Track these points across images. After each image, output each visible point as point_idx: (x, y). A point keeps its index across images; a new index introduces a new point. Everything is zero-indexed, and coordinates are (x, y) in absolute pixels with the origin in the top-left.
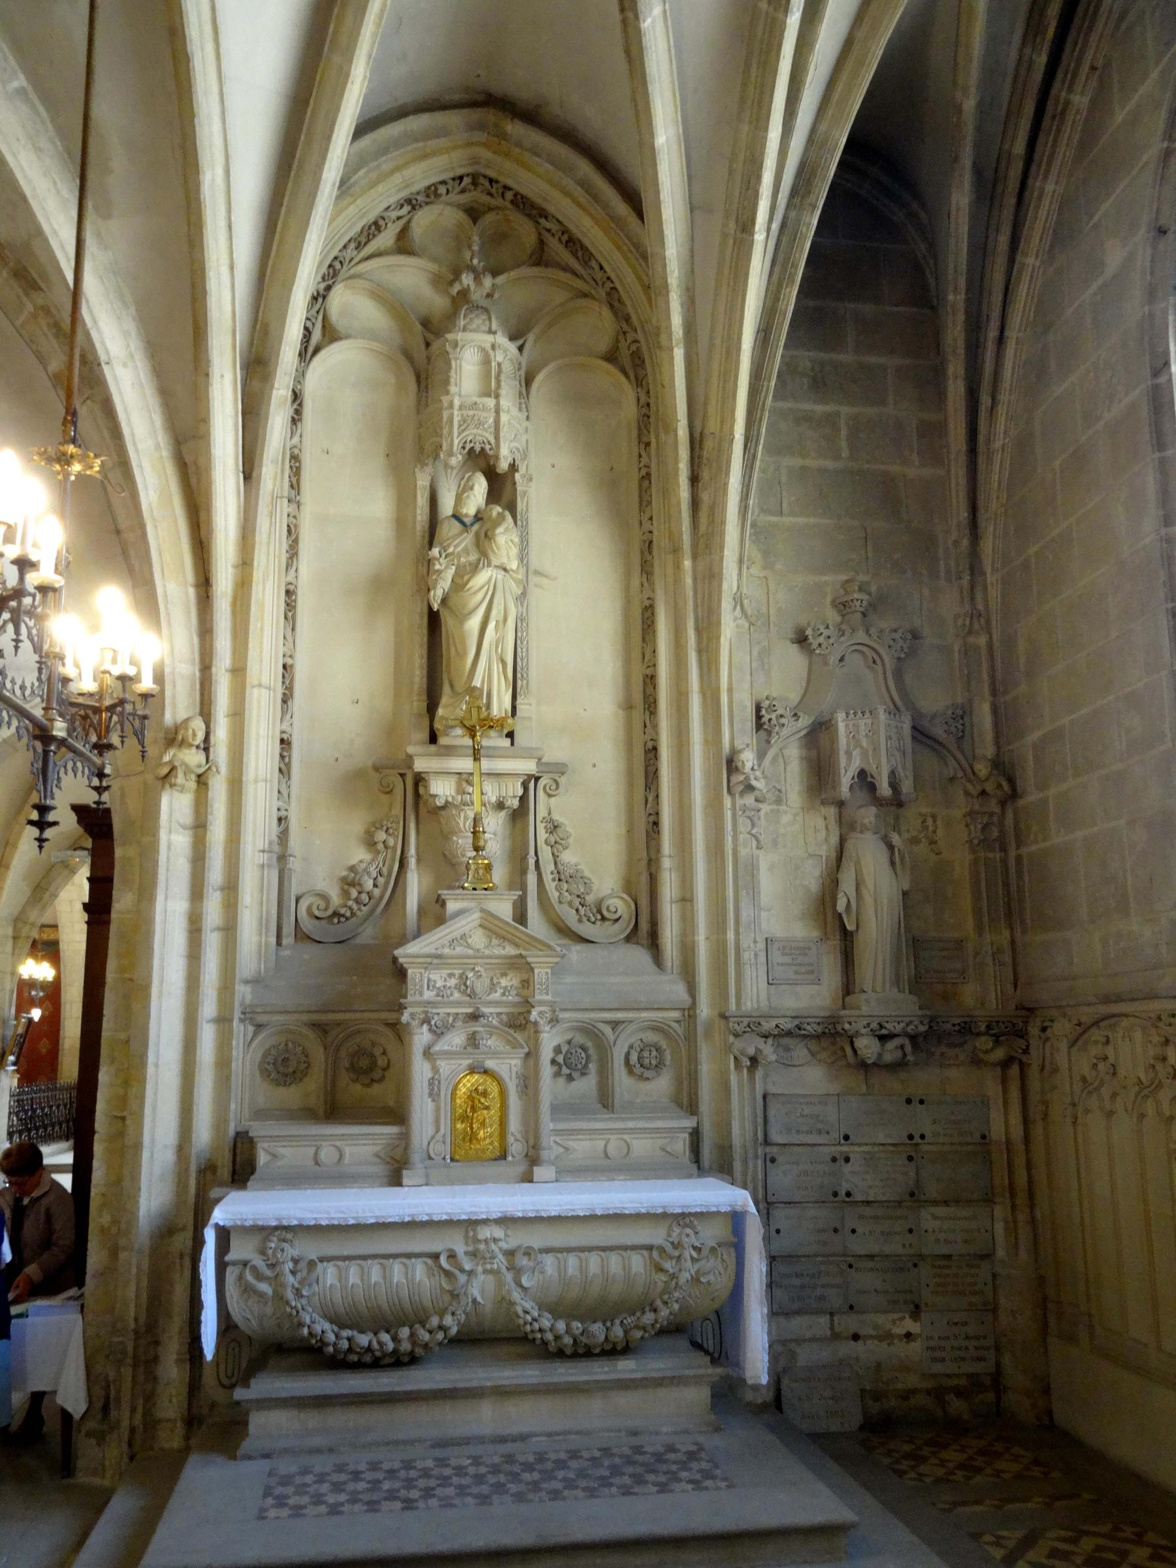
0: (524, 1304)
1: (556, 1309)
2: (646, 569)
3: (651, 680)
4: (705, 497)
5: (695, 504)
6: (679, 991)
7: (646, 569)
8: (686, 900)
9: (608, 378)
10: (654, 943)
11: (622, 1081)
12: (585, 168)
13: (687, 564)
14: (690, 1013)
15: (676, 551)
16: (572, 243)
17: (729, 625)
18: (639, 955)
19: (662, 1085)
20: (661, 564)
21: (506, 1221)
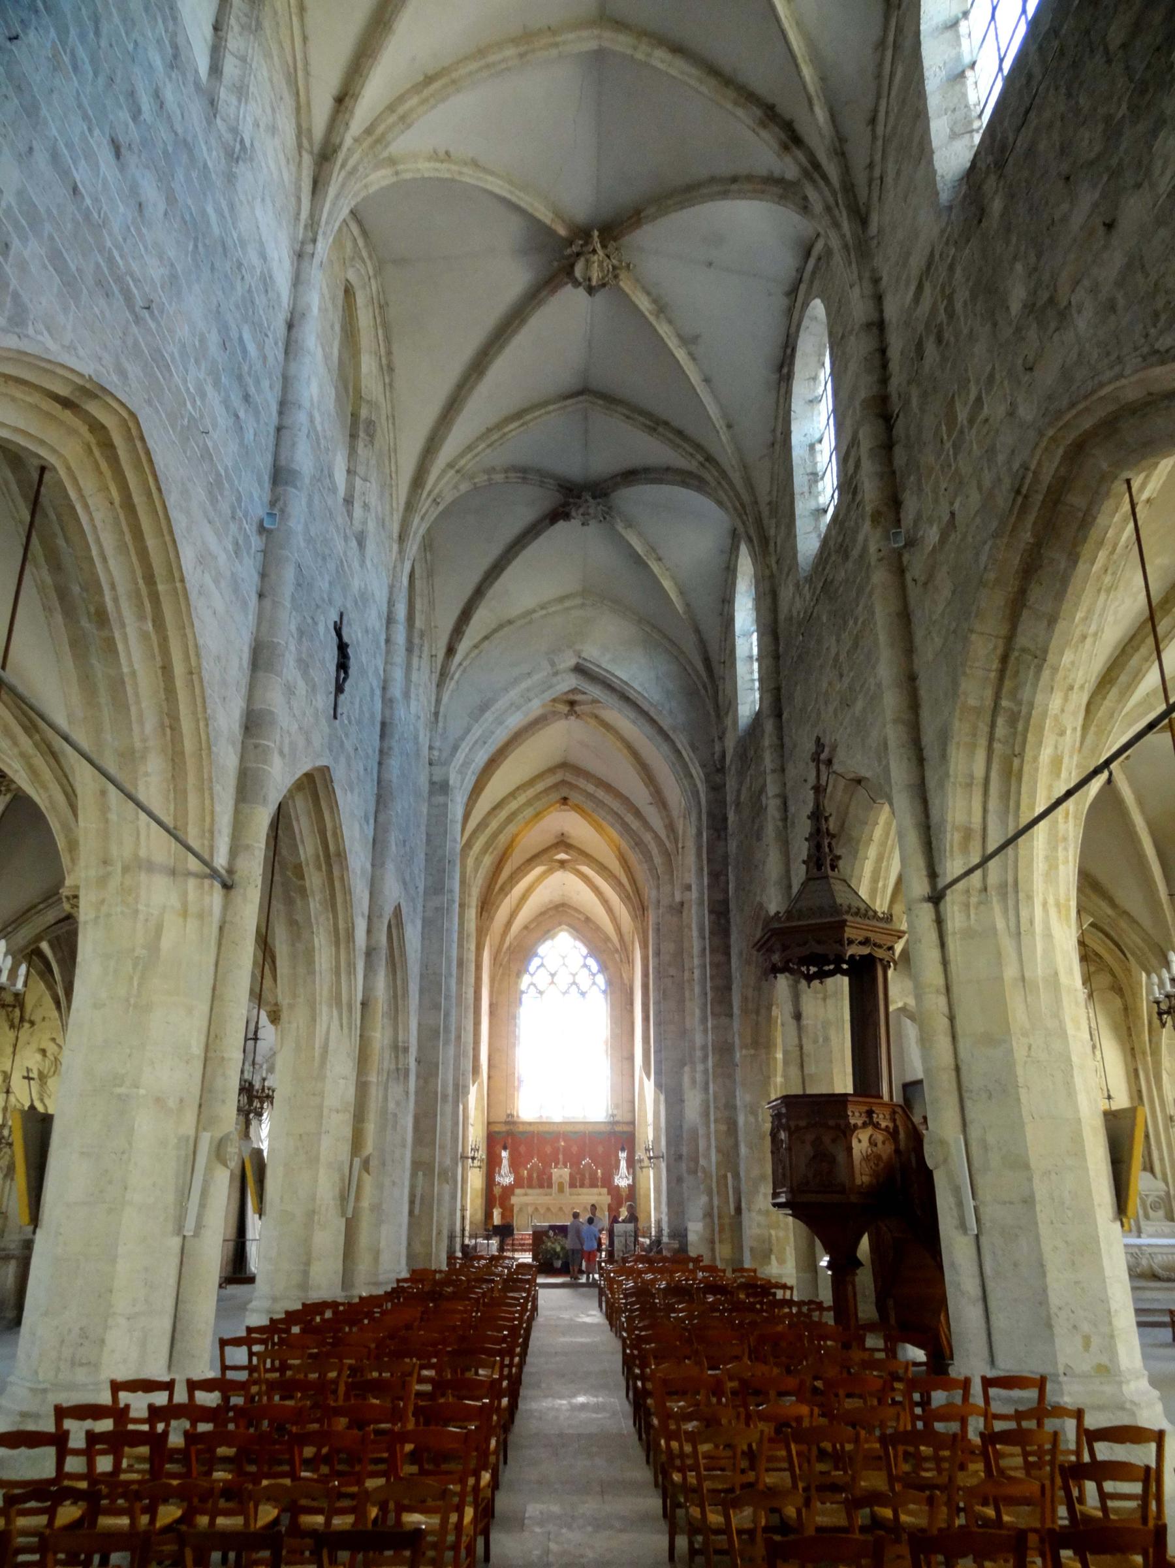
0: (1155, 1267)
1: (1163, 1268)
2: (1134, 1056)
3: (1140, 1092)
4: (1154, 1040)
5: (1150, 1041)
6: (1162, 1185)
7: (1134, 1056)
8: (1162, 1159)
9: (1111, 995)
10: (1152, 1171)
11: (1151, 1213)
12: (1100, 935)
13: (1149, 1059)
14: (1168, 1193)
15: (1144, 1053)
16: (1097, 954)
17: (1165, 1076)
18: (1148, 1175)
19: (1161, 1213)
20: (1139, 1056)
21: (1149, 1246)
